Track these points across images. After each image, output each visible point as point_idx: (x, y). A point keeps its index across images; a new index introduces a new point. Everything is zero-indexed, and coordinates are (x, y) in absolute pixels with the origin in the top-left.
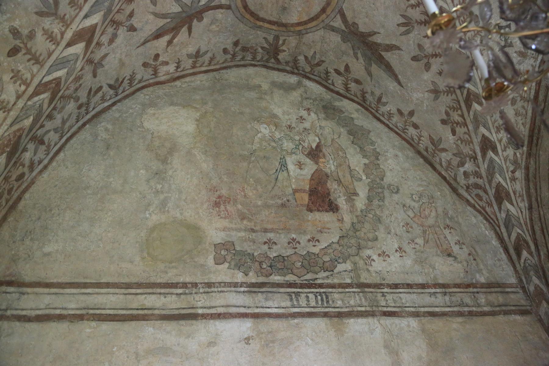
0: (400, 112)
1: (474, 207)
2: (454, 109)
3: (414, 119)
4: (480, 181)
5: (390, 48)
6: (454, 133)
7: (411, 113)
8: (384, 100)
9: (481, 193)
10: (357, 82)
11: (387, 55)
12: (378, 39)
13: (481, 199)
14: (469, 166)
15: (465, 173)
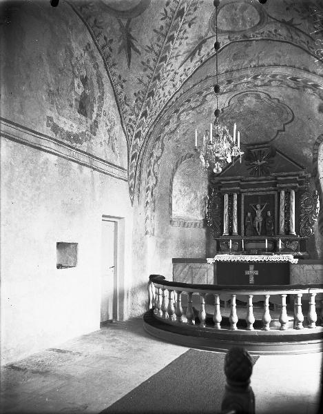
0: (120, 77)
1: (125, 133)
2: (143, 92)
3: (123, 84)
4: (134, 126)
5: (137, 51)
6: (136, 101)
7: (124, 81)
8: (117, 66)
9: (131, 130)
10: (111, 50)
11: (133, 52)
12: (134, 42)
13: (129, 131)
14: (133, 117)
15: (130, 119)
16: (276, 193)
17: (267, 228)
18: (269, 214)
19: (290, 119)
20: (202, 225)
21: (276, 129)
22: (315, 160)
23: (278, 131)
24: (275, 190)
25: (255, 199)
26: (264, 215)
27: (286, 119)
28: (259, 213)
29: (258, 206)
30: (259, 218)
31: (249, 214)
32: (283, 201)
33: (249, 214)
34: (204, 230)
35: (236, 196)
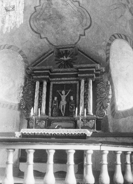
16: (78, 82)
17: (70, 110)
18: (72, 98)
19: (88, 24)
20: (17, 108)
21: (79, 33)
22: (108, 59)
23: (80, 35)
24: (77, 80)
25: (61, 87)
26: (68, 99)
27: (86, 25)
28: (64, 97)
29: (63, 92)
30: (63, 103)
31: (56, 98)
32: (83, 88)
33: (56, 98)
34: (18, 113)
35: (45, 83)
